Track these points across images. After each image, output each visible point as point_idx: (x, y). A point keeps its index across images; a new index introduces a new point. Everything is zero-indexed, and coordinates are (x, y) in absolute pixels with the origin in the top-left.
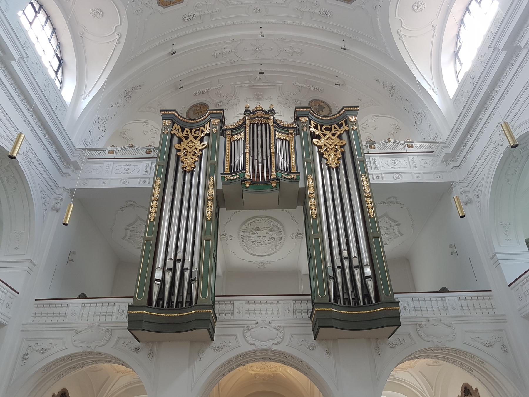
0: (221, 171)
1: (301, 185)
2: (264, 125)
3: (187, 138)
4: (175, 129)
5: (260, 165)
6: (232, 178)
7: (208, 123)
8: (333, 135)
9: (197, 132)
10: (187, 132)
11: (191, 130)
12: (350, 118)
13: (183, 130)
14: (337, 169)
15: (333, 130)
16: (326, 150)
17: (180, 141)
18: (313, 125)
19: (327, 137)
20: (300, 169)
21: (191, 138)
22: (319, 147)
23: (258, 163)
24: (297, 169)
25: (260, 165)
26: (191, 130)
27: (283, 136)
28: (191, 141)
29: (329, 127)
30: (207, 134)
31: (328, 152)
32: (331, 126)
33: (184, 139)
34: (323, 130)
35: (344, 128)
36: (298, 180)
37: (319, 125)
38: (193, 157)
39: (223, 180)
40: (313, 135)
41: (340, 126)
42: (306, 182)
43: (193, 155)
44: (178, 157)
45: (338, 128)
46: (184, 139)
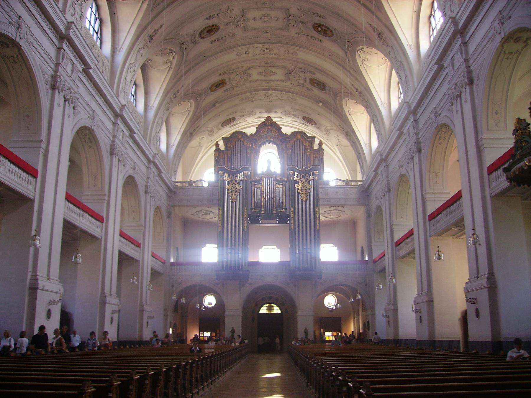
0: (250, 207)
1: (288, 213)
2: (271, 178)
3: (231, 181)
4: (226, 177)
5: (268, 203)
6: (255, 211)
7: (242, 173)
8: (306, 181)
9: (236, 177)
10: (231, 177)
11: (233, 176)
12: (315, 172)
13: (229, 175)
14: (306, 202)
15: (306, 177)
16: (301, 191)
17: (228, 184)
18: (296, 175)
19: (302, 182)
20: (287, 207)
21: (234, 181)
22: (298, 189)
23: (267, 202)
24: (286, 206)
25: (268, 203)
26: (233, 176)
27: (280, 186)
28: (234, 183)
29: (304, 175)
30: (242, 180)
31: (302, 192)
32: (305, 174)
33: (230, 183)
34: (301, 177)
35: (311, 177)
36: (286, 211)
37: (299, 174)
38: (236, 193)
39: (251, 211)
40: (296, 182)
41: (310, 175)
42: (290, 211)
43: (236, 192)
44: (228, 193)
45: (308, 177)
46: (230, 183)
